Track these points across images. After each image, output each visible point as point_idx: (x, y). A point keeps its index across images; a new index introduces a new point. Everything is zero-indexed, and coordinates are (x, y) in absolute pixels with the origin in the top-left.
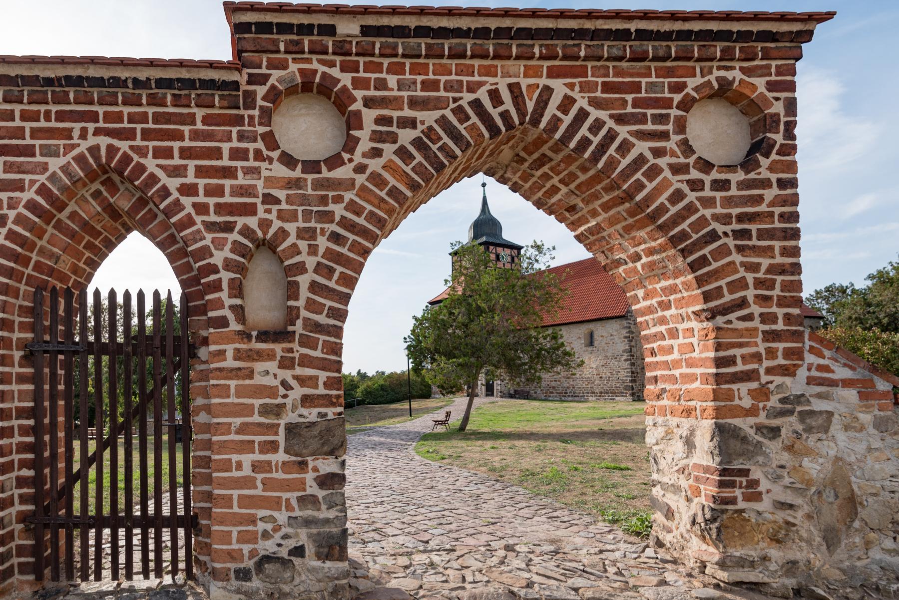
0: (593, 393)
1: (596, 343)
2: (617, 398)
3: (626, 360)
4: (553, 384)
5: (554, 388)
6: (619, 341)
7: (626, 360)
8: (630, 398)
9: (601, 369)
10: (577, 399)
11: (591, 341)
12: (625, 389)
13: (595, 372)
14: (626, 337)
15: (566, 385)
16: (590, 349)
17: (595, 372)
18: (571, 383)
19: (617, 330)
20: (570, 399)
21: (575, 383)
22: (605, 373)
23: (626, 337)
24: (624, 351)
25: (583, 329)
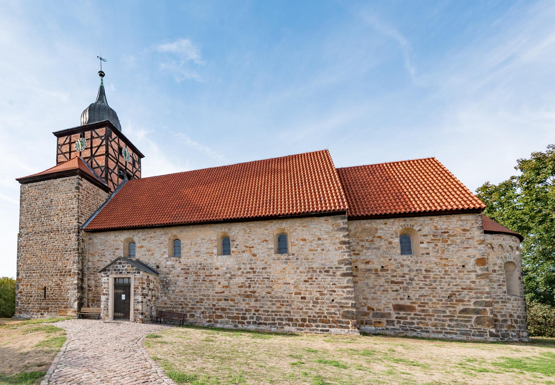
0: (291, 320)
1: (291, 249)
2: (332, 330)
3: (344, 275)
4: (222, 304)
5: (223, 309)
6: (332, 248)
7: (344, 275)
8: (357, 333)
9: (302, 286)
10: (262, 327)
11: (282, 244)
12: (344, 316)
13: (293, 290)
14: (344, 243)
15: (243, 306)
16: (284, 257)
17: (293, 290)
18: (253, 304)
19: (328, 233)
20: (252, 327)
21: (258, 304)
22: (312, 292)
23: (344, 243)
24: (340, 262)
25: (272, 230)
